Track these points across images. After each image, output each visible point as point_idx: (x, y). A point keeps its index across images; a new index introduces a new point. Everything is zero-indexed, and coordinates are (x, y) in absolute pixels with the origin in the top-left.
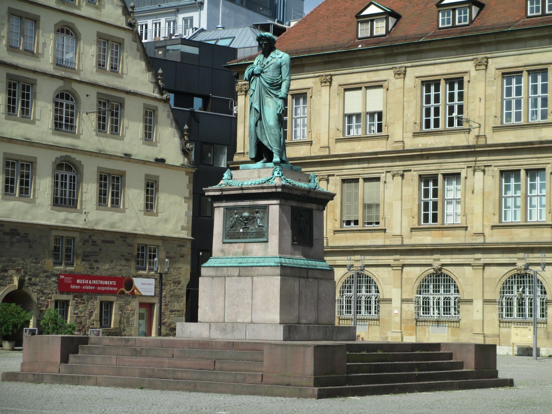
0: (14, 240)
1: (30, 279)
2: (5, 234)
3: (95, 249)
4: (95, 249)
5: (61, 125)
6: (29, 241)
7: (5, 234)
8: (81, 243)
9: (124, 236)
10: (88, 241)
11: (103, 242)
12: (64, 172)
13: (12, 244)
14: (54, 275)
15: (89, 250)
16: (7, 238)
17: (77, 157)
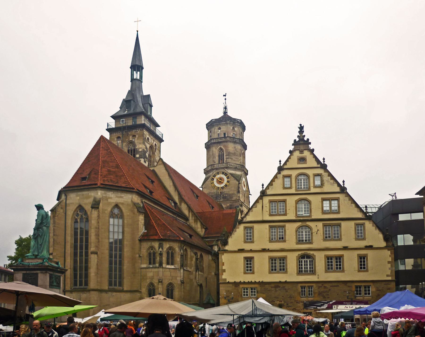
0: (277, 289)
1: (287, 304)
2: (272, 287)
3: (326, 290)
4: (326, 290)
5: (303, 241)
6: (286, 289)
7: (272, 287)
8: (317, 288)
9: (345, 282)
10: (321, 287)
11: (331, 286)
12: (306, 259)
13: (276, 291)
14: (302, 302)
15: (322, 290)
16: (273, 289)
17: (312, 252)
